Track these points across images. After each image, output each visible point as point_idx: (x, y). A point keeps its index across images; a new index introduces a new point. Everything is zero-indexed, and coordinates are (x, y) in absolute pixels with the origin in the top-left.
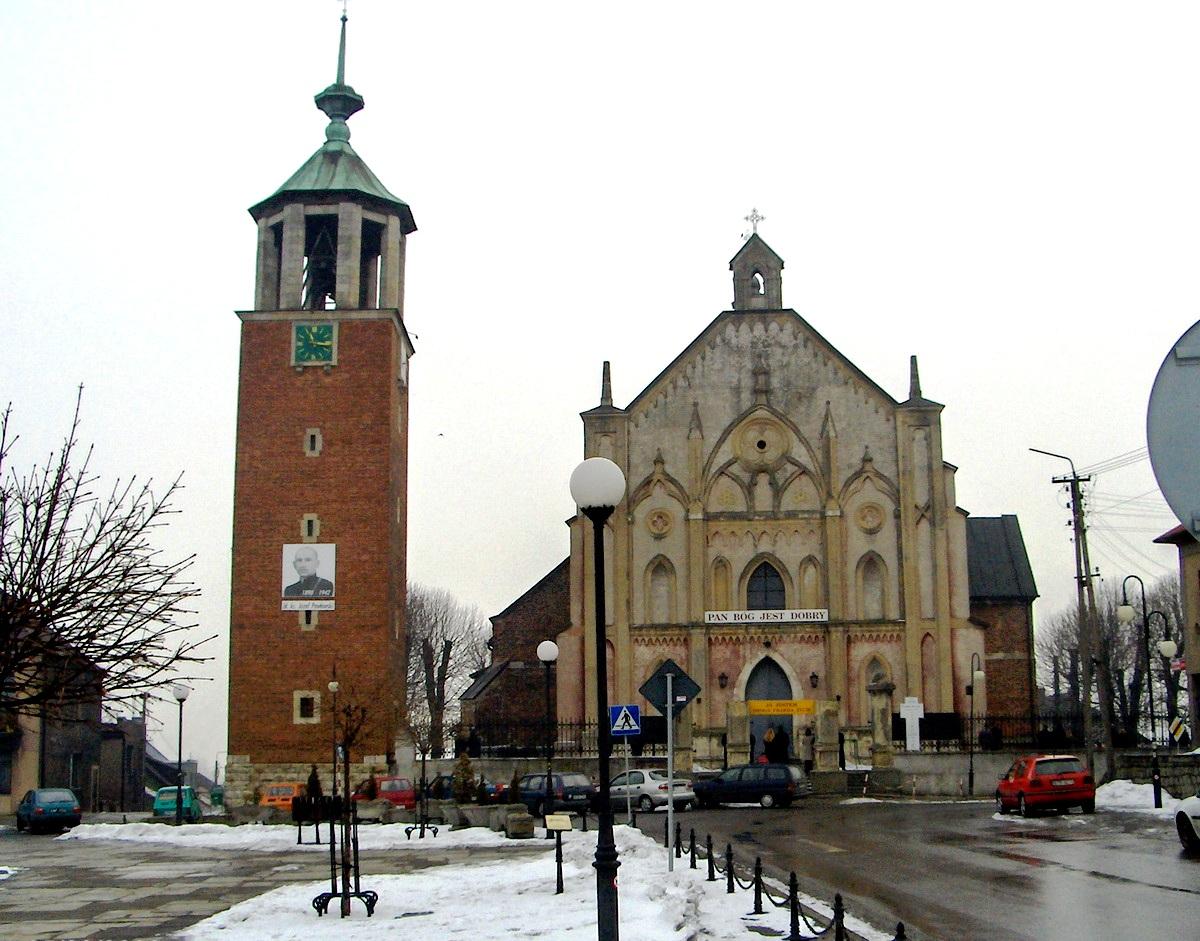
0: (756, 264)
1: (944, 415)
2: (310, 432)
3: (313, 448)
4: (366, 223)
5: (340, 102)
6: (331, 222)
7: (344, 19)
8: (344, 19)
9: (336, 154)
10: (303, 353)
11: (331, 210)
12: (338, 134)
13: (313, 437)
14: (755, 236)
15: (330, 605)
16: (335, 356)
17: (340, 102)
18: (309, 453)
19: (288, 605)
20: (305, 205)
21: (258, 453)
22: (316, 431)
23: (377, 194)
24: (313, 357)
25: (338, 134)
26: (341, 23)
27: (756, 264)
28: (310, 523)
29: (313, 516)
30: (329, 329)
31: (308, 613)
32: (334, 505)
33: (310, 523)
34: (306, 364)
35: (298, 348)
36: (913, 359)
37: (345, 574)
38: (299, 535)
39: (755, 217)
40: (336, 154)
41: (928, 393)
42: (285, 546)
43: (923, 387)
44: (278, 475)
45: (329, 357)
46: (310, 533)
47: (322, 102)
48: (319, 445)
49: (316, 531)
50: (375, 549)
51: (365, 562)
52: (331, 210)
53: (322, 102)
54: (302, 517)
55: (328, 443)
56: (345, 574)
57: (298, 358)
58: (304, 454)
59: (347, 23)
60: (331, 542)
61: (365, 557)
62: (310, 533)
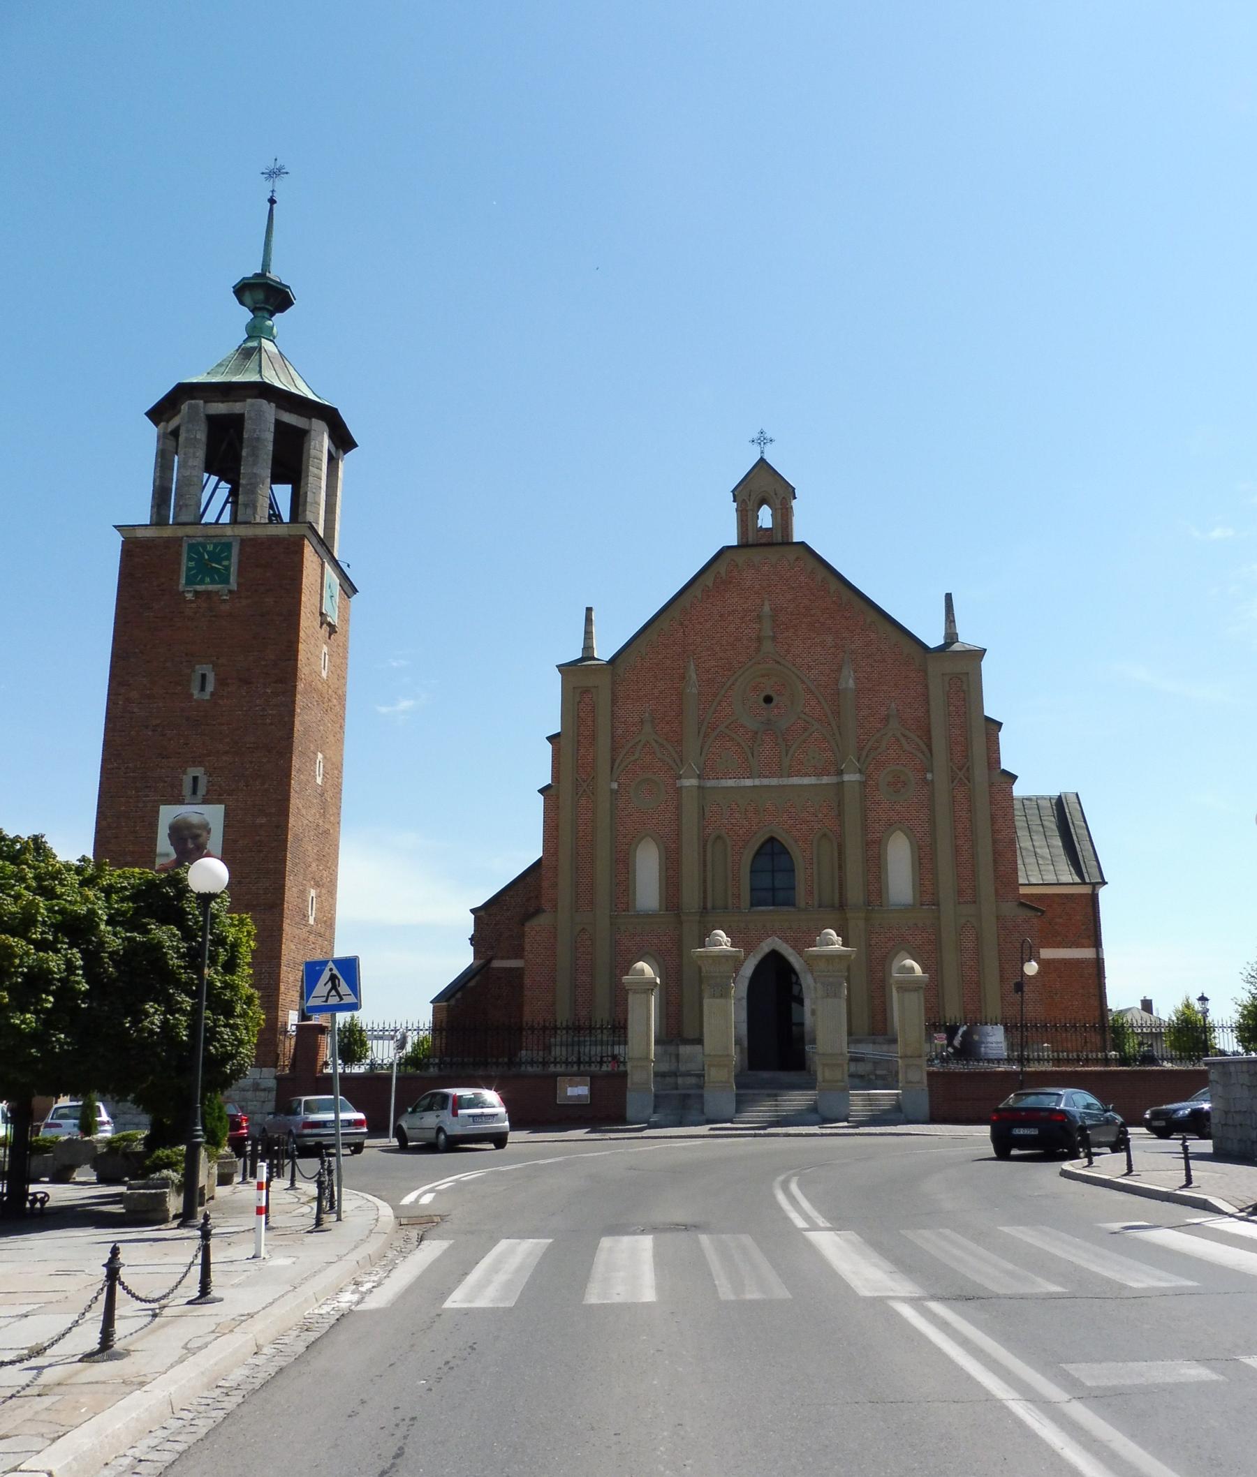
0: (763, 488)
1: (986, 664)
2: (200, 669)
3: (203, 688)
4: (278, 423)
6: (237, 422)
7: (272, 201)
8: (272, 201)
10: (195, 576)
11: (237, 407)
13: (204, 676)
14: (762, 460)
16: (233, 579)
17: (265, 296)
18: (196, 694)
20: (206, 402)
21: (134, 695)
22: (207, 669)
23: (294, 390)
27: (763, 488)
28: (195, 779)
29: (198, 771)
30: (228, 546)
32: (224, 758)
33: (195, 779)
34: (199, 588)
35: (189, 569)
36: (949, 597)
37: (235, 841)
39: (762, 440)
41: (968, 637)
42: (162, 807)
43: (960, 628)
44: (158, 722)
45: (227, 581)
46: (194, 792)
47: (242, 290)
48: (210, 687)
49: (202, 790)
50: (273, 810)
51: (261, 826)
52: (237, 407)
53: (242, 290)
54: (184, 773)
55: (221, 682)
56: (235, 841)
57: (190, 581)
58: (192, 695)
60: (220, 803)
61: (264, 820)
62: (194, 792)
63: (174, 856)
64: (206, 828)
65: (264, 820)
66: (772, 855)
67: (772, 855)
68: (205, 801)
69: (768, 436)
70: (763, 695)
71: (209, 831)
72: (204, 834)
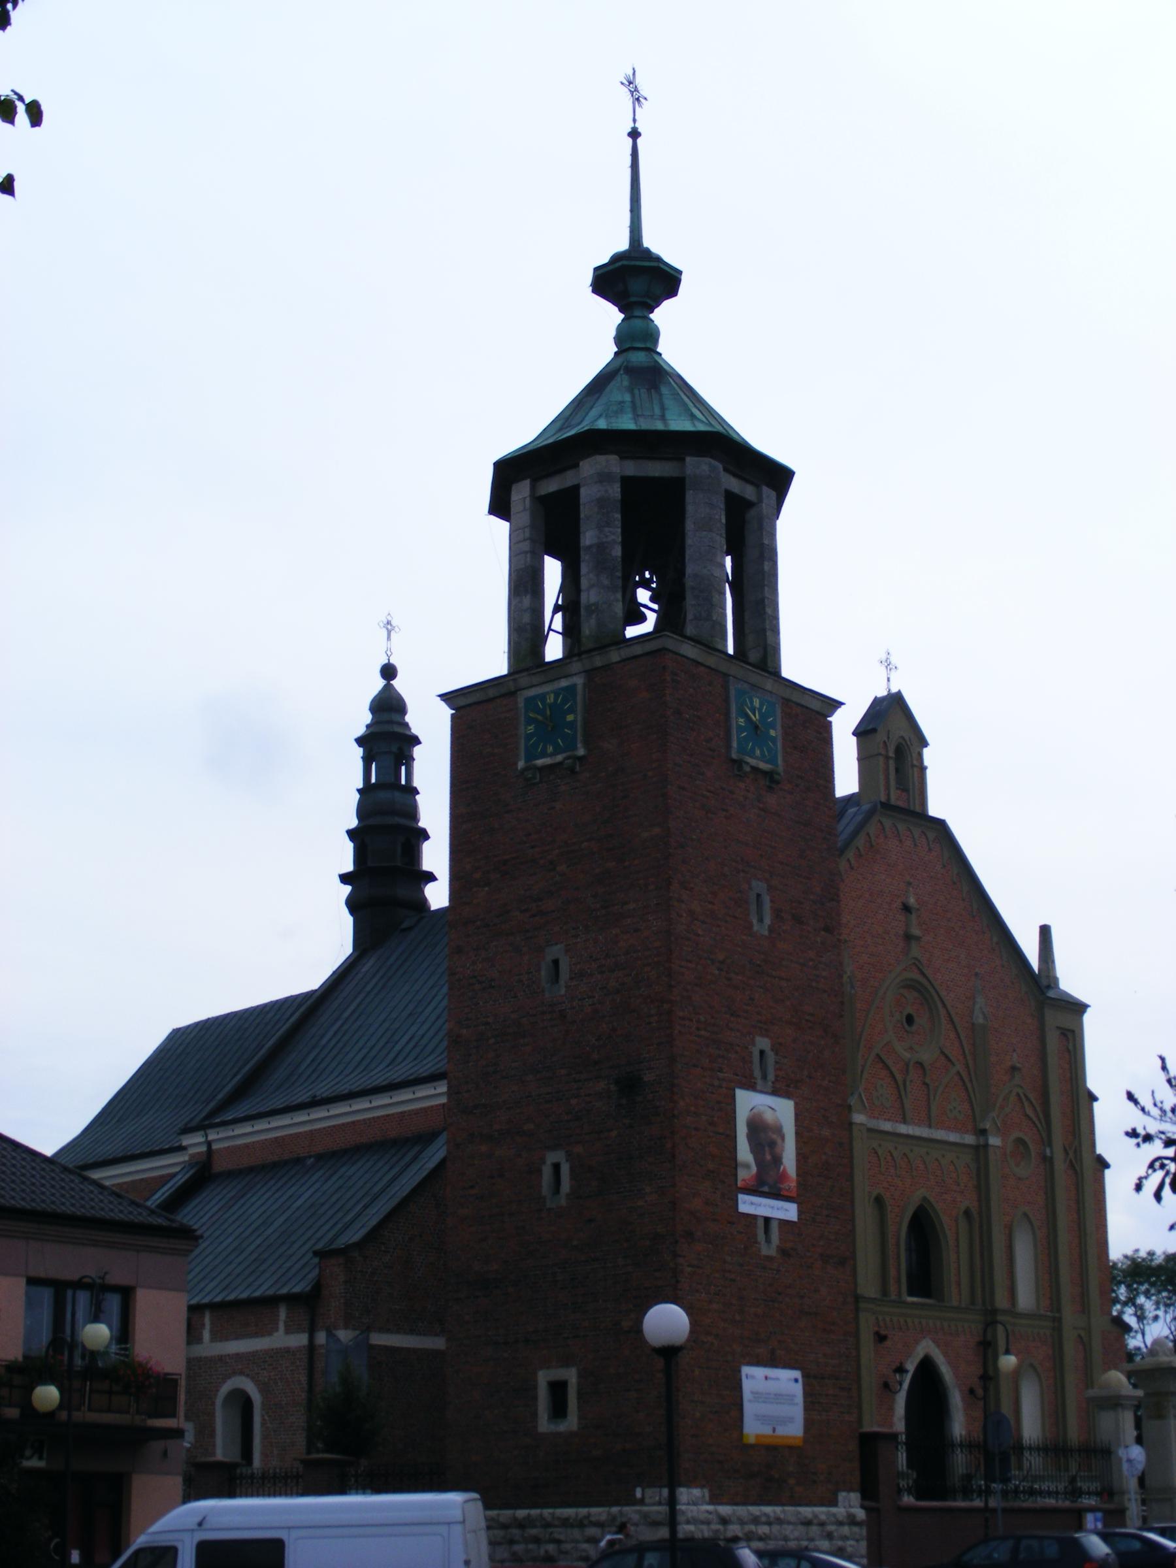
5: (636, 281)
7: (634, 134)
8: (634, 134)
9: (637, 364)
12: (636, 340)
15: (788, 1211)
17: (636, 281)
19: (748, 1205)
24: (758, 752)
25: (636, 340)
26: (630, 141)
31: (767, 1220)
38: (752, 1076)
40: (637, 364)
45: (773, 761)
46: (764, 1077)
55: (777, 914)
59: (639, 141)
61: (826, 1132)
62: (764, 1077)
63: (754, 1169)
64: (779, 1130)
65: (826, 1132)
66: (922, 1226)
67: (922, 1226)
68: (775, 1092)
69: (884, 659)
70: (905, 1013)
71: (783, 1138)
72: (779, 1141)
